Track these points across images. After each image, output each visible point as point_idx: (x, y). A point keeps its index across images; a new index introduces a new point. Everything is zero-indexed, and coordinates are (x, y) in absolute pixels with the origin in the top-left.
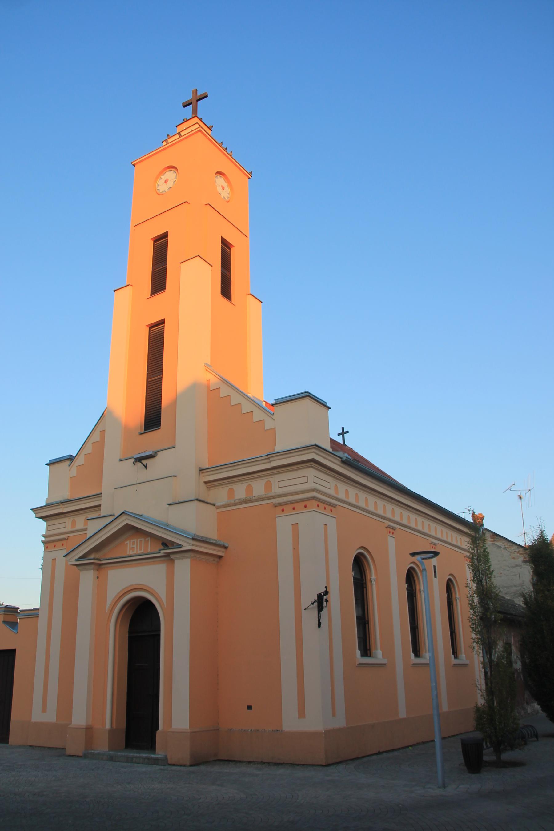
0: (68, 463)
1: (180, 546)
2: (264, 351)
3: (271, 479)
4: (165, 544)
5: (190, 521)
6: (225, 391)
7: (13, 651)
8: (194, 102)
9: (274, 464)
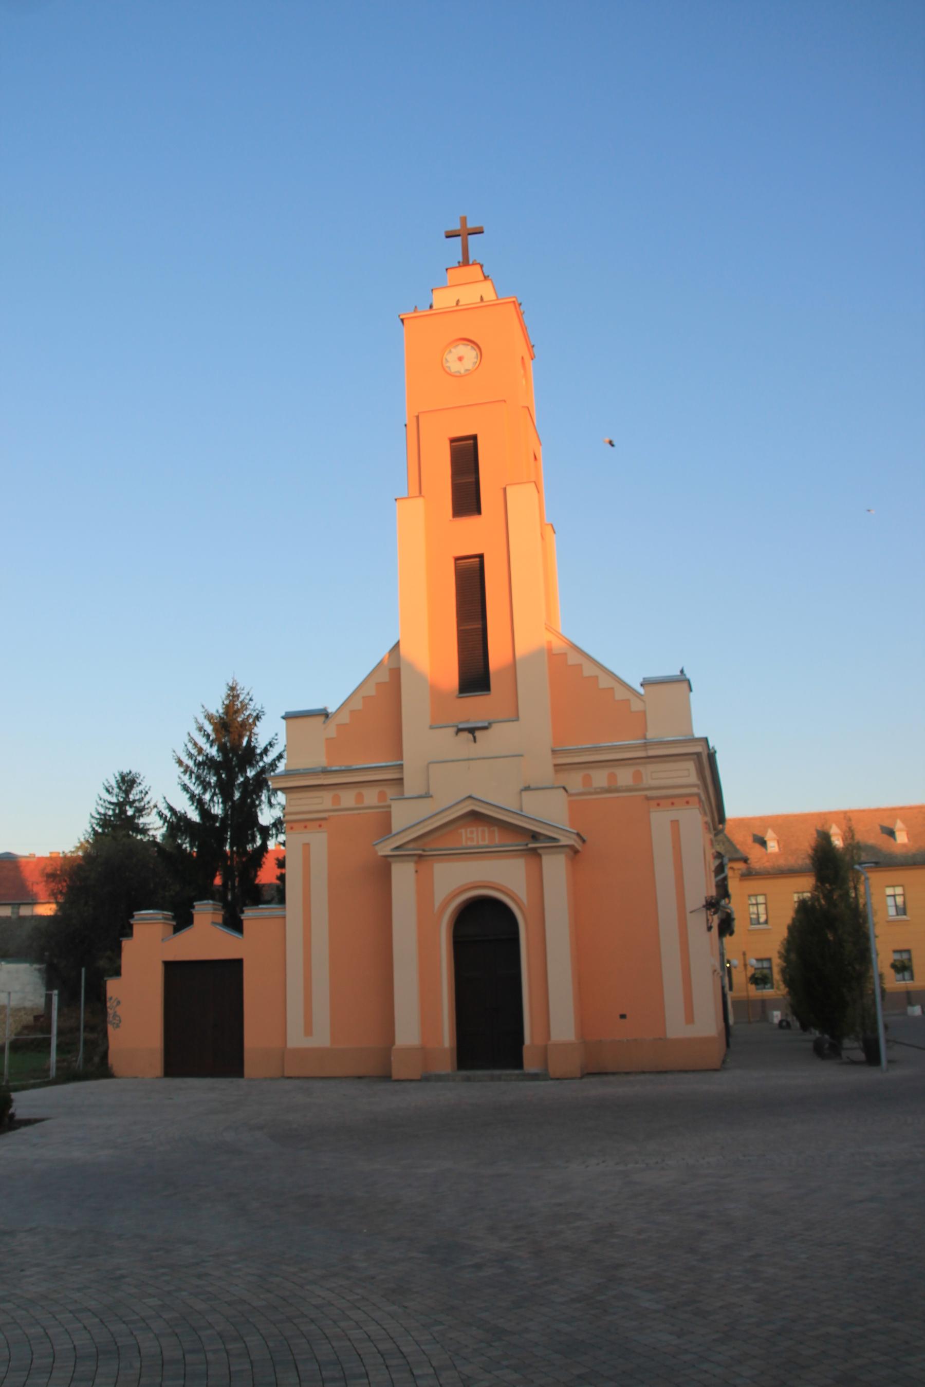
0: (322, 719)
1: (554, 839)
3: (641, 769)
4: (535, 836)
5: (550, 811)
6: (573, 659)
7: (239, 962)
8: (464, 233)
9: (651, 753)
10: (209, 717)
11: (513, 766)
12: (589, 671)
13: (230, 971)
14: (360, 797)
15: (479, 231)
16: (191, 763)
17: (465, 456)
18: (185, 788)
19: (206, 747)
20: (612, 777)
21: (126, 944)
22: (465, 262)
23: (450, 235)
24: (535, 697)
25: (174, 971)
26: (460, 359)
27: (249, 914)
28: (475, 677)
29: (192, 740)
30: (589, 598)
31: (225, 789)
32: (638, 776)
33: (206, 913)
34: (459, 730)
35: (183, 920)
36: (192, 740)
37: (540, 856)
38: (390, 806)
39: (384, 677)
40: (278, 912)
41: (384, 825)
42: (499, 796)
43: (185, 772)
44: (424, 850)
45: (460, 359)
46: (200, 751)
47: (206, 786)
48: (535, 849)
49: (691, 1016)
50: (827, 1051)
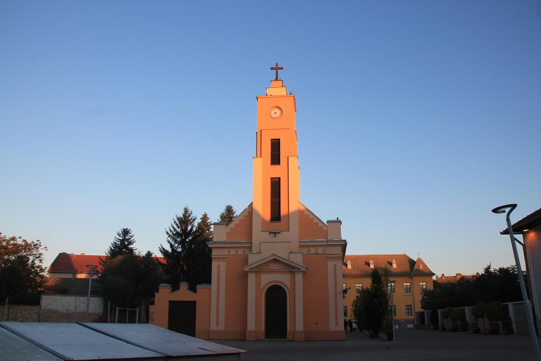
2: (310, 194)
4: (294, 267)
5: (297, 259)
9: (329, 244)
10: (178, 219)
11: (287, 244)
12: (316, 221)
14: (237, 252)
15: (282, 68)
16: (171, 233)
17: (276, 145)
18: (169, 242)
20: (317, 250)
21: (157, 295)
22: (277, 79)
23: (272, 69)
24: (294, 225)
25: (172, 304)
26: (275, 113)
27: (199, 287)
28: (276, 215)
29: (172, 226)
31: (182, 243)
32: (324, 250)
33: (184, 286)
34: (270, 233)
35: (175, 287)
36: (172, 226)
39: (246, 214)
40: (209, 287)
41: (245, 260)
42: (282, 254)
43: (169, 237)
44: (259, 270)
45: (275, 113)
46: (175, 230)
47: (176, 241)
49: (336, 325)
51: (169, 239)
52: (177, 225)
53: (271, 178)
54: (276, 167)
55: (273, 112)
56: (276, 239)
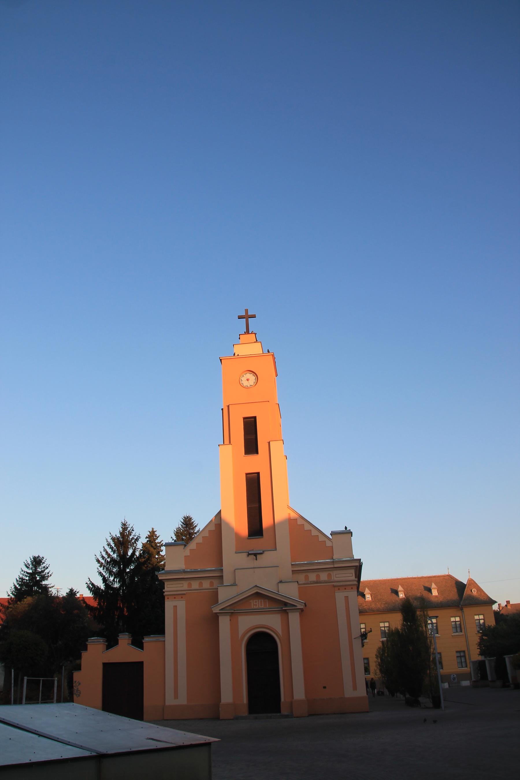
3: (331, 573)
4: (286, 604)
5: (290, 592)
6: (300, 522)
7: (142, 663)
9: (336, 566)
10: (113, 539)
11: (274, 571)
12: (314, 533)
13: (136, 669)
14: (201, 584)
15: (254, 316)
16: (103, 561)
17: (250, 426)
18: (100, 574)
19: (112, 553)
20: (318, 576)
21: (85, 655)
22: (247, 332)
23: (240, 317)
24: (283, 540)
25: (107, 666)
27: (146, 639)
28: (256, 528)
29: (105, 550)
30: (307, 493)
31: (120, 575)
32: (329, 576)
33: (124, 639)
34: (249, 554)
35: (112, 642)
36: (105, 550)
37: (288, 613)
38: (217, 589)
39: (213, 528)
40: (161, 639)
41: (214, 597)
42: (268, 585)
43: (101, 566)
44: (234, 610)
45: (248, 380)
46: (109, 555)
47: (111, 573)
48: (285, 610)
50: (413, 703)
51: (101, 569)
52: (112, 548)
53: (247, 474)
54: (252, 458)
55: (244, 379)
56: (257, 563)
